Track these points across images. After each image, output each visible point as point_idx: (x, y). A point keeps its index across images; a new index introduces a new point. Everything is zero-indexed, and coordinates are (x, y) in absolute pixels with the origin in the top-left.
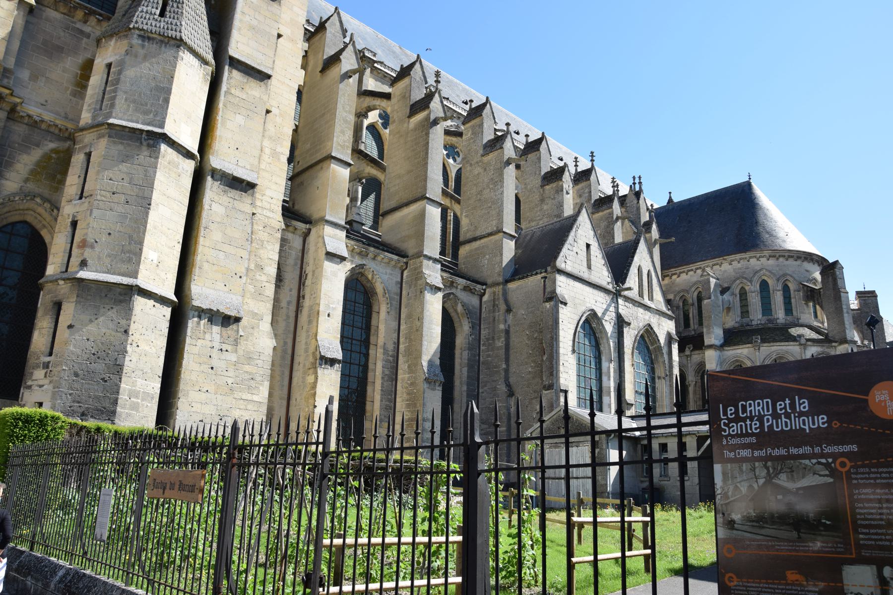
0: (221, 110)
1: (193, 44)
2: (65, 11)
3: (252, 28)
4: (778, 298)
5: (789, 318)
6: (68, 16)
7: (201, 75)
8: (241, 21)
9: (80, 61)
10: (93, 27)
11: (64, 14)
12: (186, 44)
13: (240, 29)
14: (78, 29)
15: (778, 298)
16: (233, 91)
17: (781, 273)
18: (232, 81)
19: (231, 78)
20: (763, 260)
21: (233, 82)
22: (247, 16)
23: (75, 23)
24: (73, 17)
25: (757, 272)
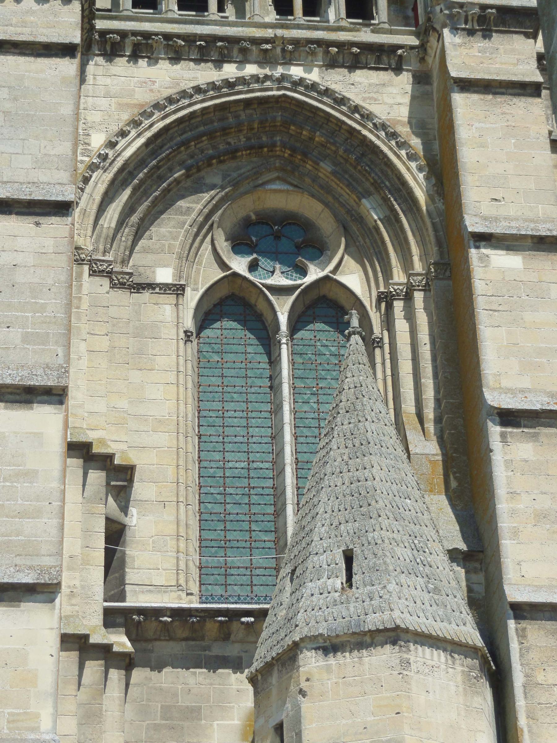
0: (526, 730)
1: (423, 620)
2: (186, 634)
6: (194, 639)
7: (459, 678)
8: (513, 513)
9: (236, 722)
10: (242, 642)
11: (186, 639)
12: (407, 631)
13: (516, 533)
14: (217, 657)
16: (540, 677)
18: (531, 655)
19: (528, 649)
21: (533, 656)
22: (524, 496)
23: (208, 648)
24: (202, 638)
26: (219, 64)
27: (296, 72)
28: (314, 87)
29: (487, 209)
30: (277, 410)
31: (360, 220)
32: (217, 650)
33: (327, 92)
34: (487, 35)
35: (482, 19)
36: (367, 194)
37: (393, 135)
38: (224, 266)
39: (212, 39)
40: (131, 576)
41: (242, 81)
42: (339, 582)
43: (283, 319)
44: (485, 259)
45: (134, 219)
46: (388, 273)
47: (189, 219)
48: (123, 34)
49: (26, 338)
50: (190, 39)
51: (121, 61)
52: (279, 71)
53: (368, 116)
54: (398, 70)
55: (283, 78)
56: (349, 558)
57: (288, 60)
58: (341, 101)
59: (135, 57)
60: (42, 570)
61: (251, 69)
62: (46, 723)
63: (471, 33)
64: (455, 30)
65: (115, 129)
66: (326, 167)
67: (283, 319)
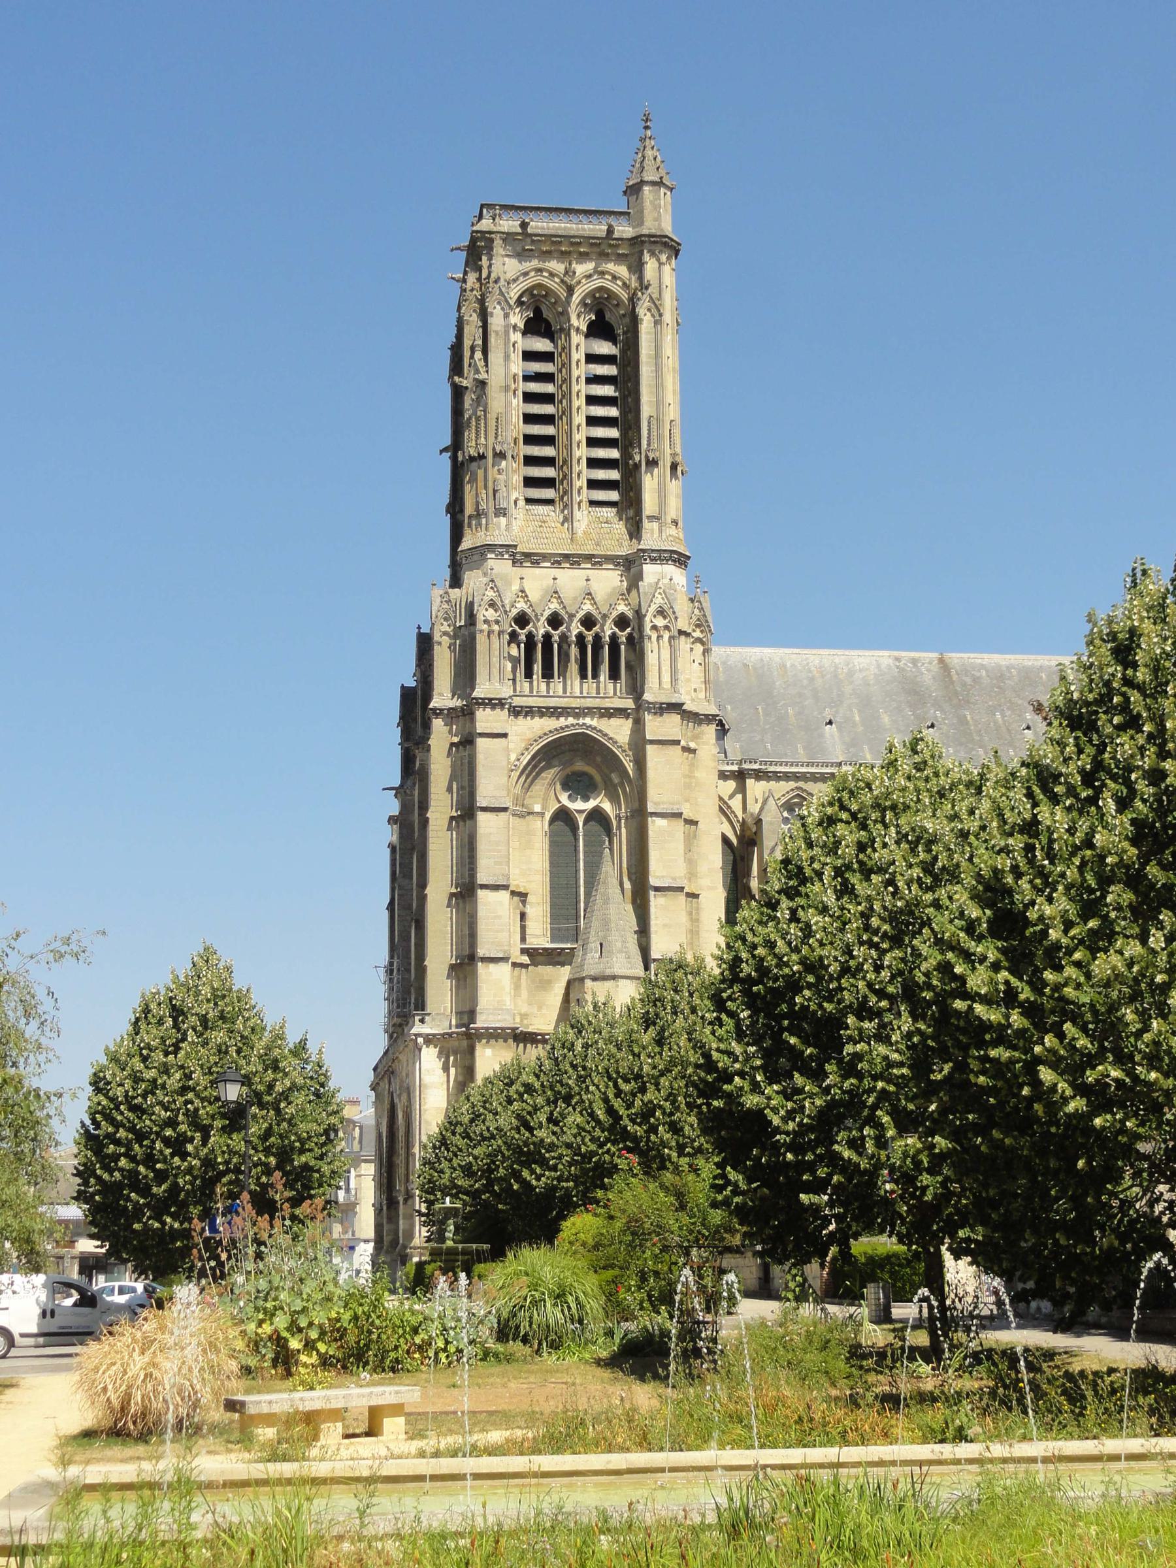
3: (665, 925)
26: (558, 718)
27: (588, 721)
28: (595, 728)
30: (577, 861)
31: (611, 780)
32: (557, 959)
33: (600, 731)
34: (661, 715)
35: (661, 708)
36: (612, 771)
37: (624, 751)
38: (559, 802)
39: (556, 708)
40: (528, 931)
41: (567, 726)
42: (598, 955)
43: (581, 824)
44: (653, 822)
45: (526, 785)
46: (620, 809)
47: (546, 782)
48: (521, 707)
49: (496, 863)
50: (548, 708)
51: (521, 718)
52: (581, 721)
53: (616, 742)
54: (627, 718)
55: (584, 724)
56: (601, 945)
57: (585, 715)
58: (606, 735)
59: (526, 716)
60: (505, 952)
61: (571, 720)
62: (508, 1003)
63: (655, 713)
64: (649, 712)
65: (519, 751)
66: (599, 759)
67: (581, 824)
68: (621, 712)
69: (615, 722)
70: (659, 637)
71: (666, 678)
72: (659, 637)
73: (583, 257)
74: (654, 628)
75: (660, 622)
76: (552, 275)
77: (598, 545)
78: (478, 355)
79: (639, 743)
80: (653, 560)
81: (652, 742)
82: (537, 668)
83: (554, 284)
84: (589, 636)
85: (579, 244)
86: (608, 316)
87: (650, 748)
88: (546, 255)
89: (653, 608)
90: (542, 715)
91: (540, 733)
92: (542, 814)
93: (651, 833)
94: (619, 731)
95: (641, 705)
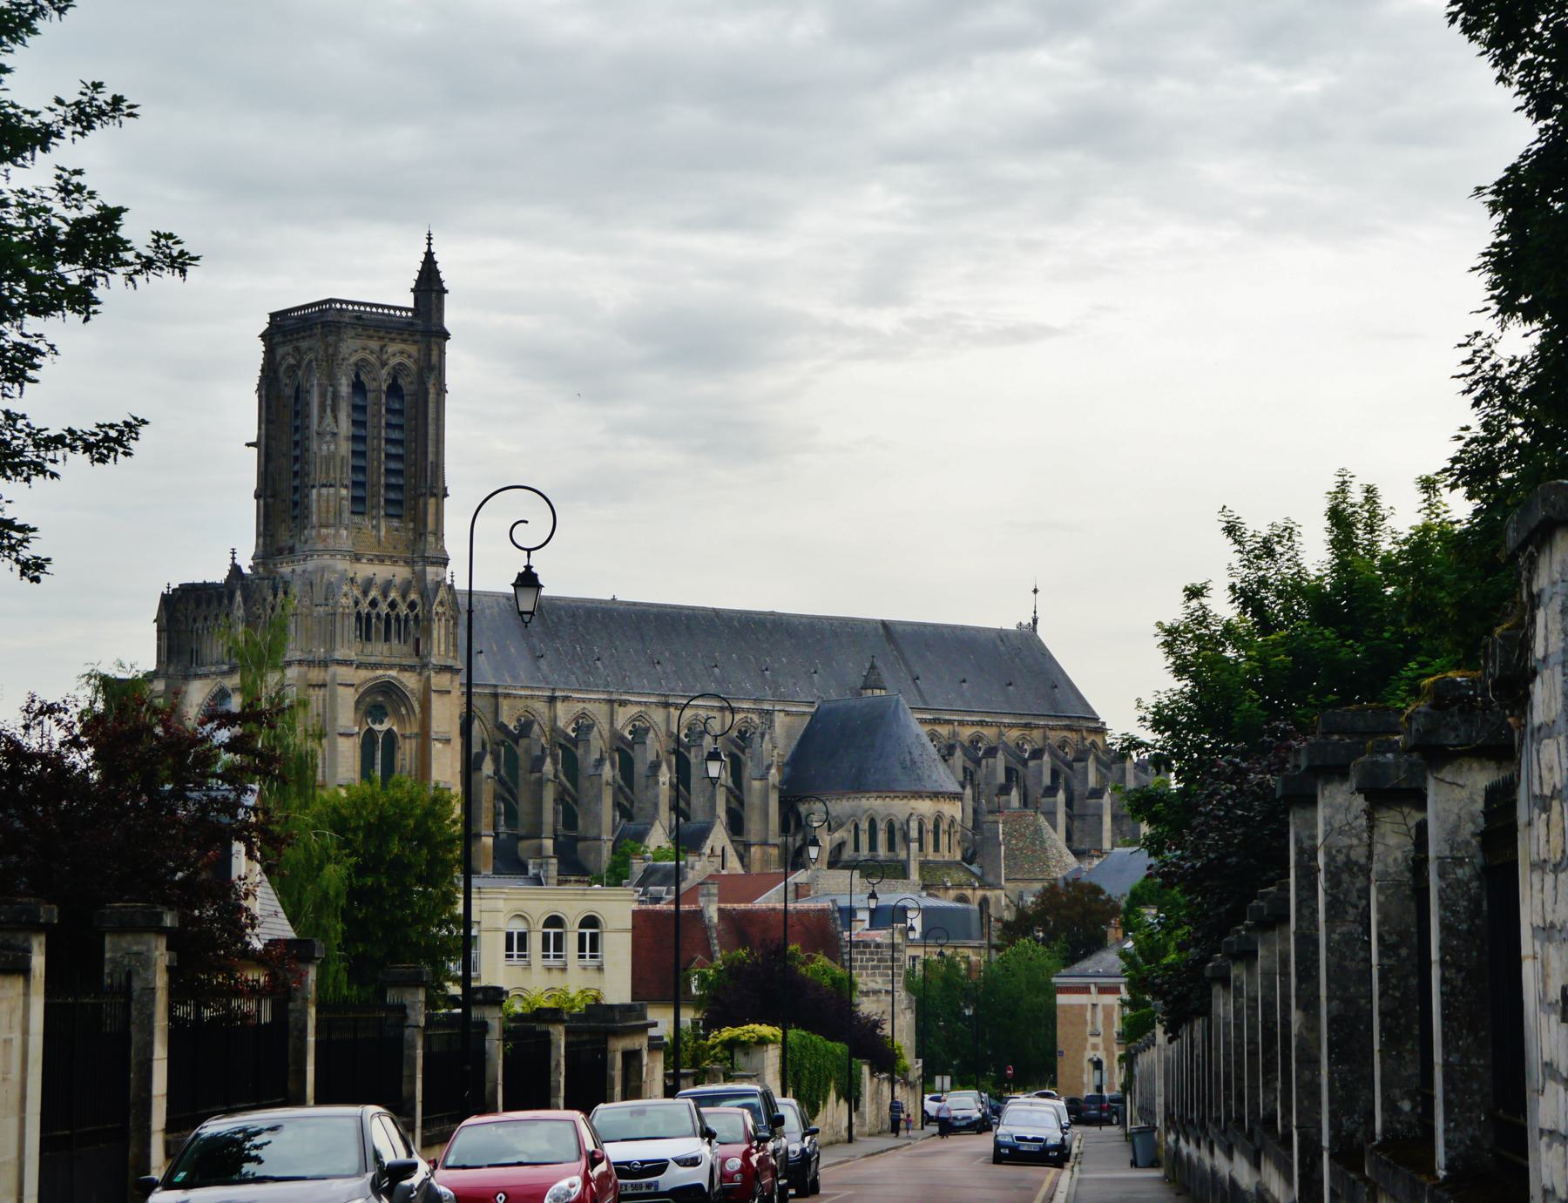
4: (882, 837)
5: (891, 854)
15: (882, 837)
17: (886, 813)
20: (872, 800)
25: (868, 810)
29: (436, 733)
68: (411, 668)
69: (407, 674)
70: (439, 620)
71: (443, 647)
72: (439, 620)
73: (392, 340)
74: (437, 613)
75: (440, 610)
76: (372, 352)
77: (395, 548)
78: (329, 410)
79: (427, 691)
80: (433, 564)
81: (435, 691)
82: (364, 637)
83: (372, 358)
84: (393, 614)
85: (390, 333)
86: (400, 381)
87: (434, 696)
88: (370, 337)
89: (438, 600)
90: (366, 668)
91: (363, 680)
92: (358, 733)
93: (433, 753)
94: (410, 681)
95: (425, 666)
